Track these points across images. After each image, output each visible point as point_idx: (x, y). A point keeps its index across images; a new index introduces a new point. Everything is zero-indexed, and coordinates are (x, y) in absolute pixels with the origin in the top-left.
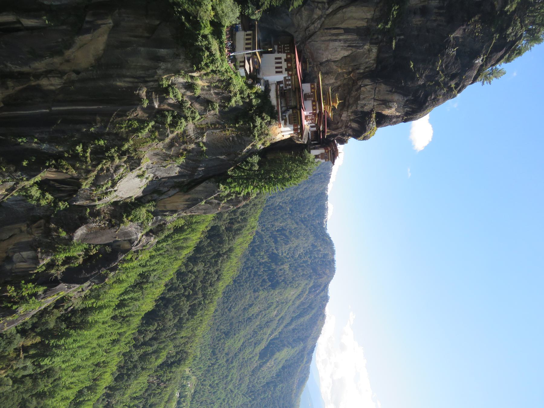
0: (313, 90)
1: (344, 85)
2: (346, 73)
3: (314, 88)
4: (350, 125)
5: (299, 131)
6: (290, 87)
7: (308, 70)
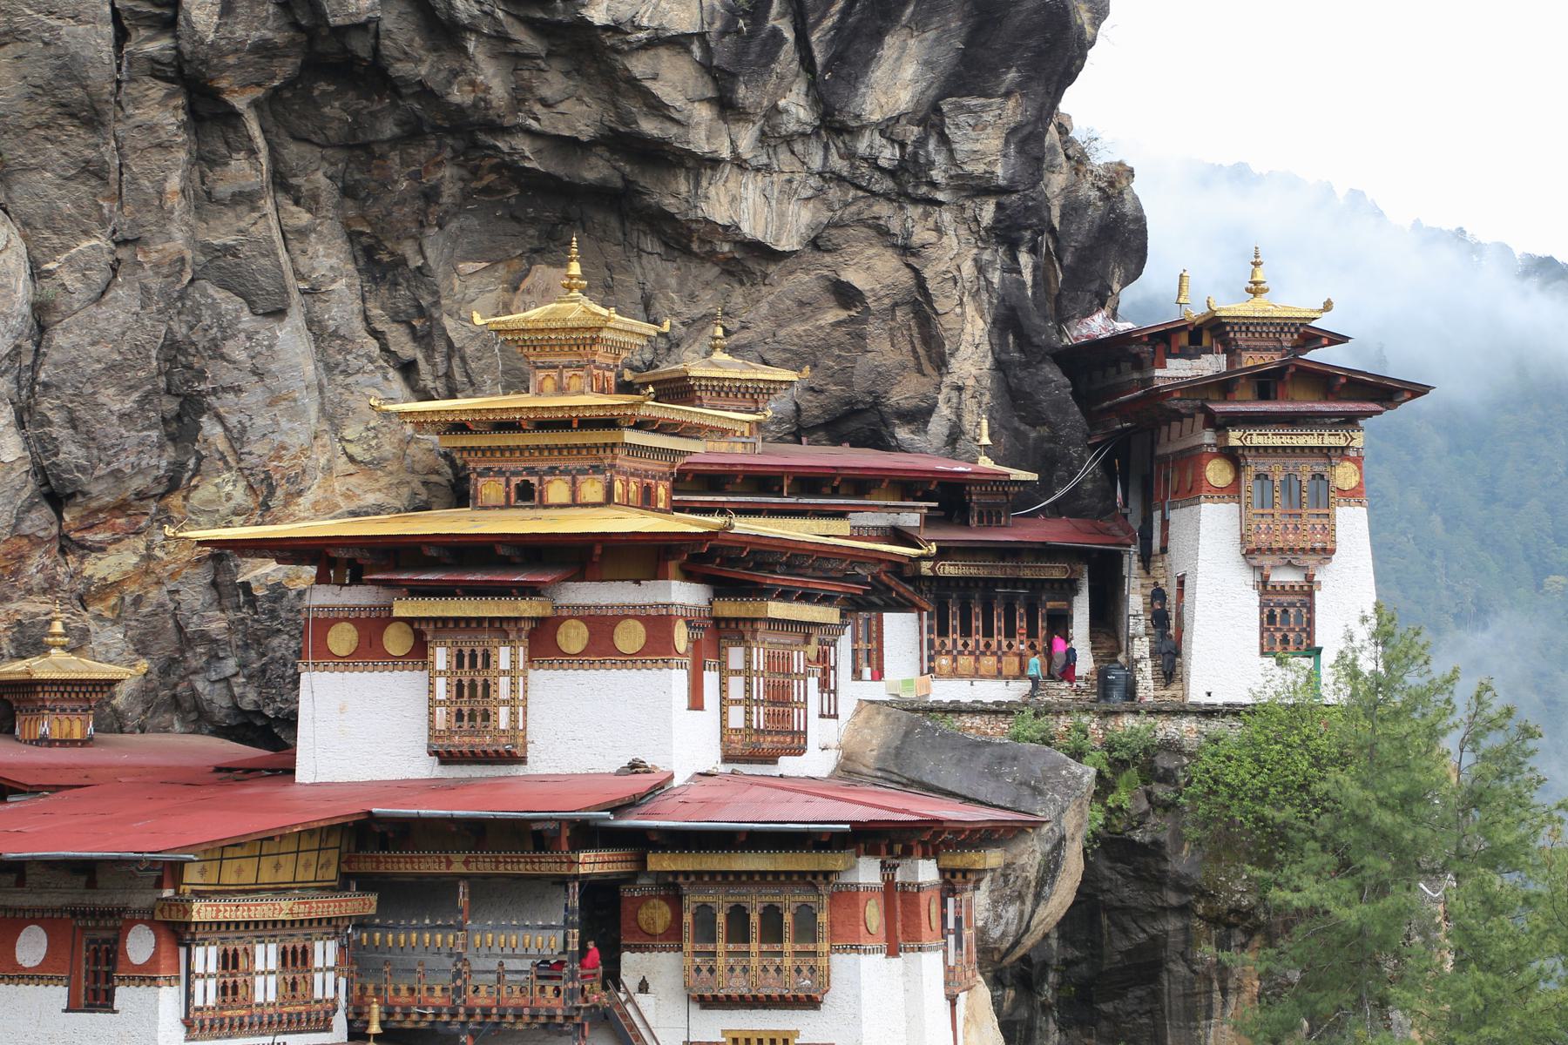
0: (396, 641)
1: (348, 191)
2: (205, 160)
3: (371, 627)
4: (886, 129)
5: (927, 872)
6: (325, 952)
7: (113, 661)
